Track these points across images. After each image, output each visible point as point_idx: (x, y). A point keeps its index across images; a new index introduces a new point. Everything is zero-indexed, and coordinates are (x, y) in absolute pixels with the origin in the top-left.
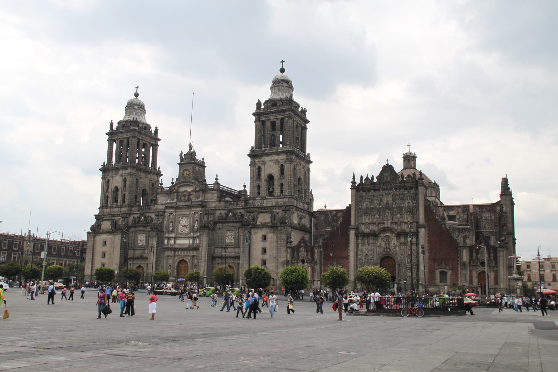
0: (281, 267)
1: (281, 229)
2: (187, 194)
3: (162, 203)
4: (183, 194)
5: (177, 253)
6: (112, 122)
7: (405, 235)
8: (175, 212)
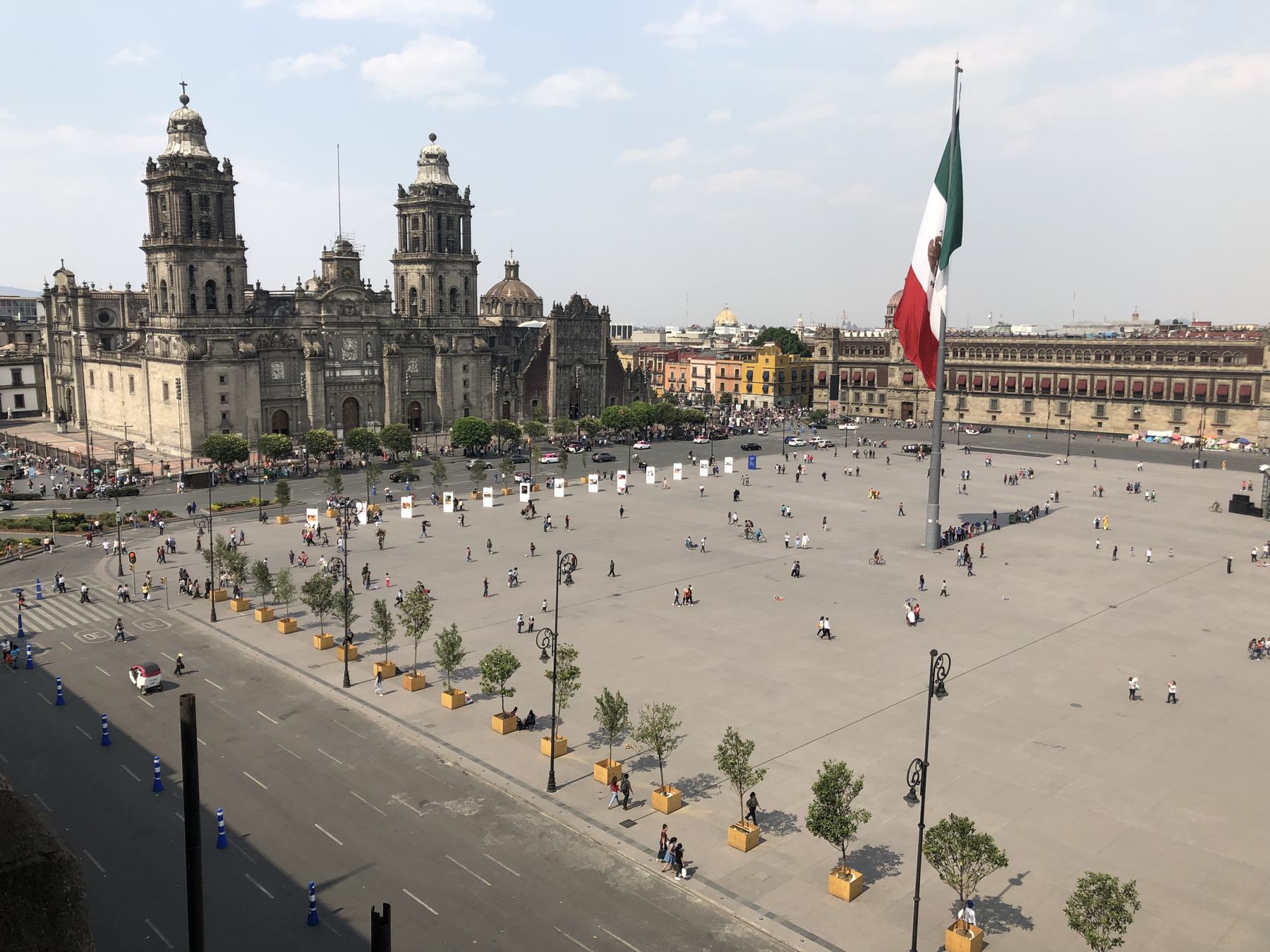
2: (352, 305)
3: (308, 314)
5: (342, 389)
8: (338, 330)
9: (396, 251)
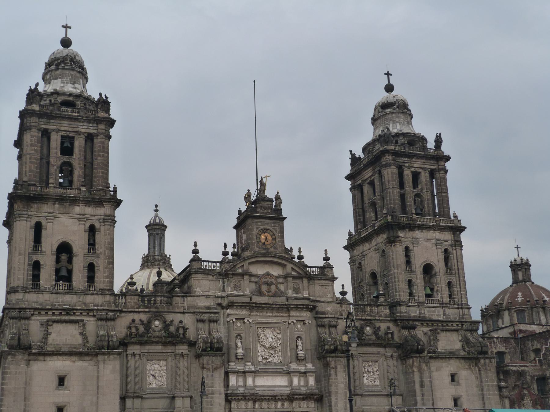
1: (485, 363)
2: (273, 281)
3: (207, 293)
4: (264, 280)
6: (36, 88)
9: (350, 234)
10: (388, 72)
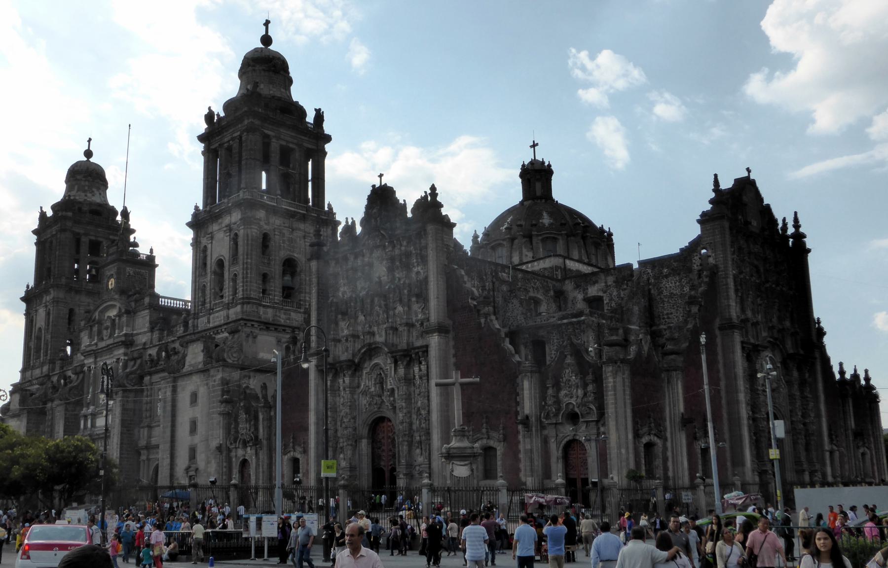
0: (213, 461)
7: (405, 356)
10: (267, 20)
